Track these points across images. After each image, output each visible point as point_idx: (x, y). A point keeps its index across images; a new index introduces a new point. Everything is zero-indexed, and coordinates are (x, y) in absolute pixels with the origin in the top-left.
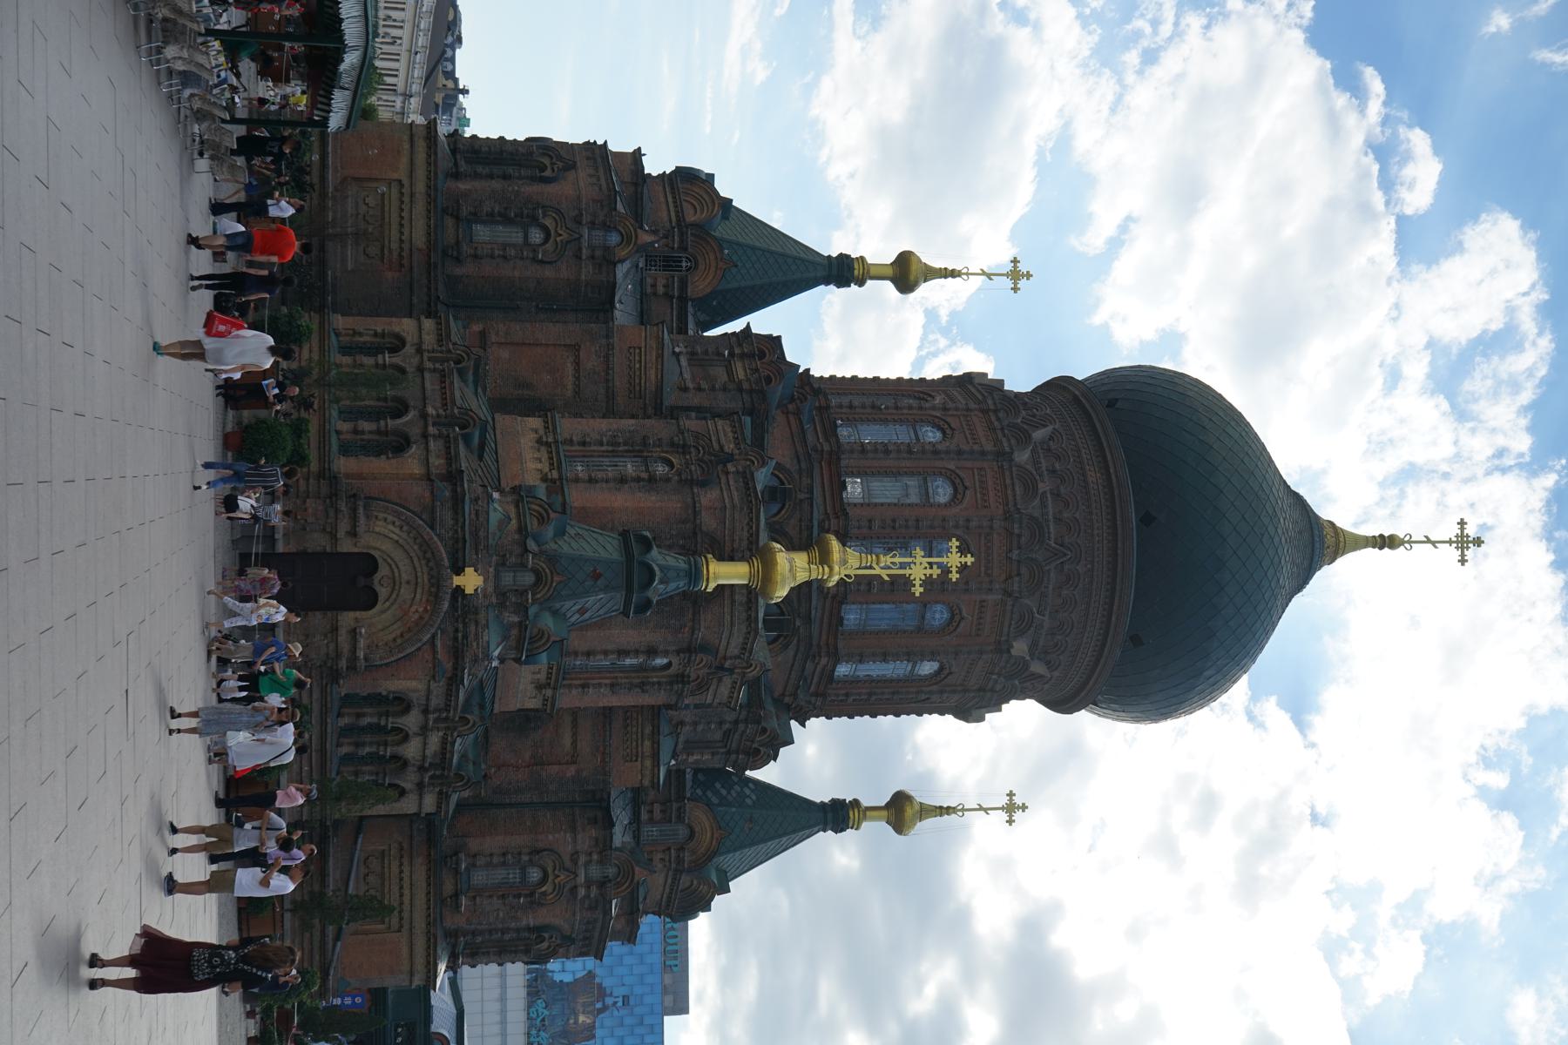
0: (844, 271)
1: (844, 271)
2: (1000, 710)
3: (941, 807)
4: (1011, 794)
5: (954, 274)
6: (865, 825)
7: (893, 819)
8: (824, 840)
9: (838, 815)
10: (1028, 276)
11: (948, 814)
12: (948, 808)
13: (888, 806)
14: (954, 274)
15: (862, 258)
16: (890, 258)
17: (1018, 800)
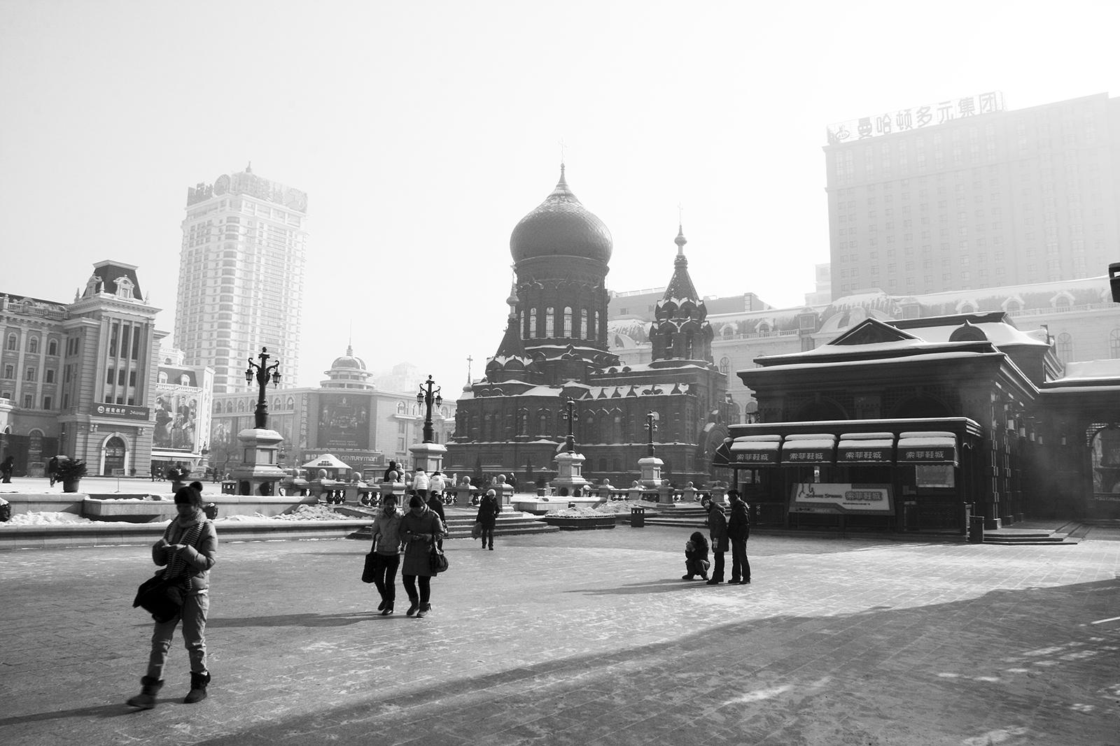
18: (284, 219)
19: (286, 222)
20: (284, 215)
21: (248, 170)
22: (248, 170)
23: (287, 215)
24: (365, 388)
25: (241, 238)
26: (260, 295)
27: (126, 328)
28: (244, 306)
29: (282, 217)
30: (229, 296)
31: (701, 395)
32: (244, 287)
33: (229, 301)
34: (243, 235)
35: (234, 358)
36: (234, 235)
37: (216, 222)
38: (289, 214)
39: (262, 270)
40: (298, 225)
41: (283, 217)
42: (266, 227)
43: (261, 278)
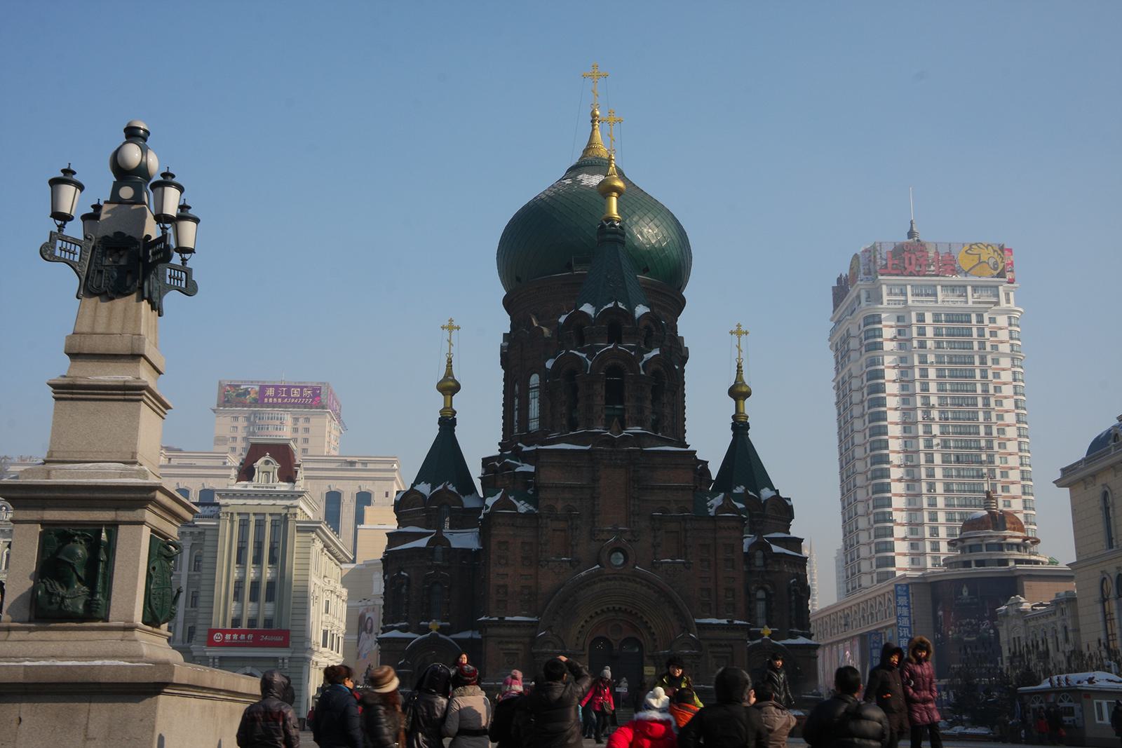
0: (447, 422)
1: (447, 422)
2: (682, 338)
3: (737, 371)
4: (732, 333)
5: (450, 362)
6: (747, 412)
7: (742, 397)
8: (752, 435)
9: (740, 427)
10: (451, 320)
11: (741, 367)
12: (738, 366)
13: (736, 400)
14: (450, 362)
15: (440, 412)
16: (440, 397)
17: (735, 329)
18: (966, 296)
19: (970, 300)
20: (966, 292)
21: (911, 234)
22: (911, 234)
23: (969, 289)
24: (1012, 564)
25: (888, 346)
26: (936, 430)
27: (260, 525)
28: (909, 453)
29: (959, 296)
30: (880, 440)
31: (560, 506)
32: (904, 423)
33: (881, 448)
34: (892, 340)
35: (904, 539)
36: (875, 343)
37: (854, 331)
38: (975, 288)
39: (933, 387)
40: (994, 300)
41: (964, 294)
42: (929, 318)
43: (934, 400)
